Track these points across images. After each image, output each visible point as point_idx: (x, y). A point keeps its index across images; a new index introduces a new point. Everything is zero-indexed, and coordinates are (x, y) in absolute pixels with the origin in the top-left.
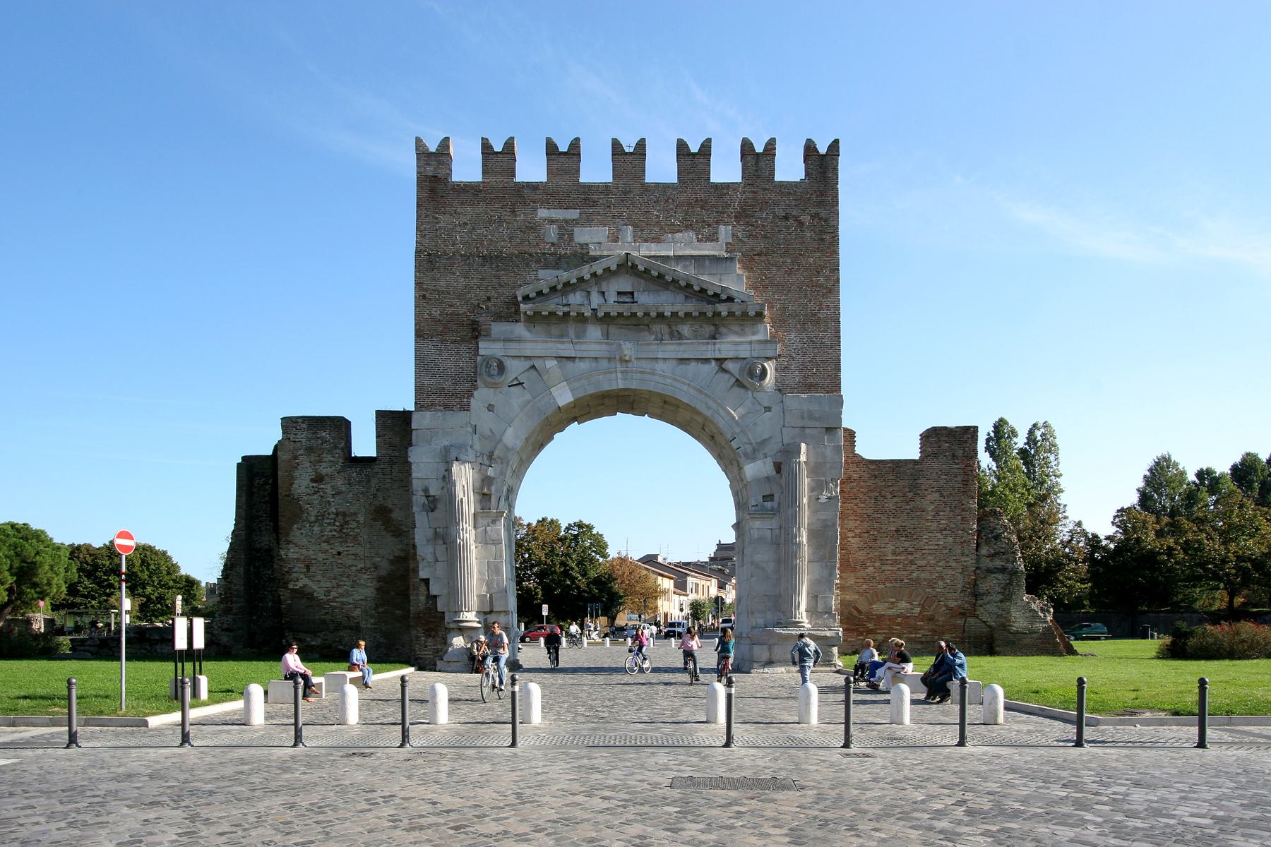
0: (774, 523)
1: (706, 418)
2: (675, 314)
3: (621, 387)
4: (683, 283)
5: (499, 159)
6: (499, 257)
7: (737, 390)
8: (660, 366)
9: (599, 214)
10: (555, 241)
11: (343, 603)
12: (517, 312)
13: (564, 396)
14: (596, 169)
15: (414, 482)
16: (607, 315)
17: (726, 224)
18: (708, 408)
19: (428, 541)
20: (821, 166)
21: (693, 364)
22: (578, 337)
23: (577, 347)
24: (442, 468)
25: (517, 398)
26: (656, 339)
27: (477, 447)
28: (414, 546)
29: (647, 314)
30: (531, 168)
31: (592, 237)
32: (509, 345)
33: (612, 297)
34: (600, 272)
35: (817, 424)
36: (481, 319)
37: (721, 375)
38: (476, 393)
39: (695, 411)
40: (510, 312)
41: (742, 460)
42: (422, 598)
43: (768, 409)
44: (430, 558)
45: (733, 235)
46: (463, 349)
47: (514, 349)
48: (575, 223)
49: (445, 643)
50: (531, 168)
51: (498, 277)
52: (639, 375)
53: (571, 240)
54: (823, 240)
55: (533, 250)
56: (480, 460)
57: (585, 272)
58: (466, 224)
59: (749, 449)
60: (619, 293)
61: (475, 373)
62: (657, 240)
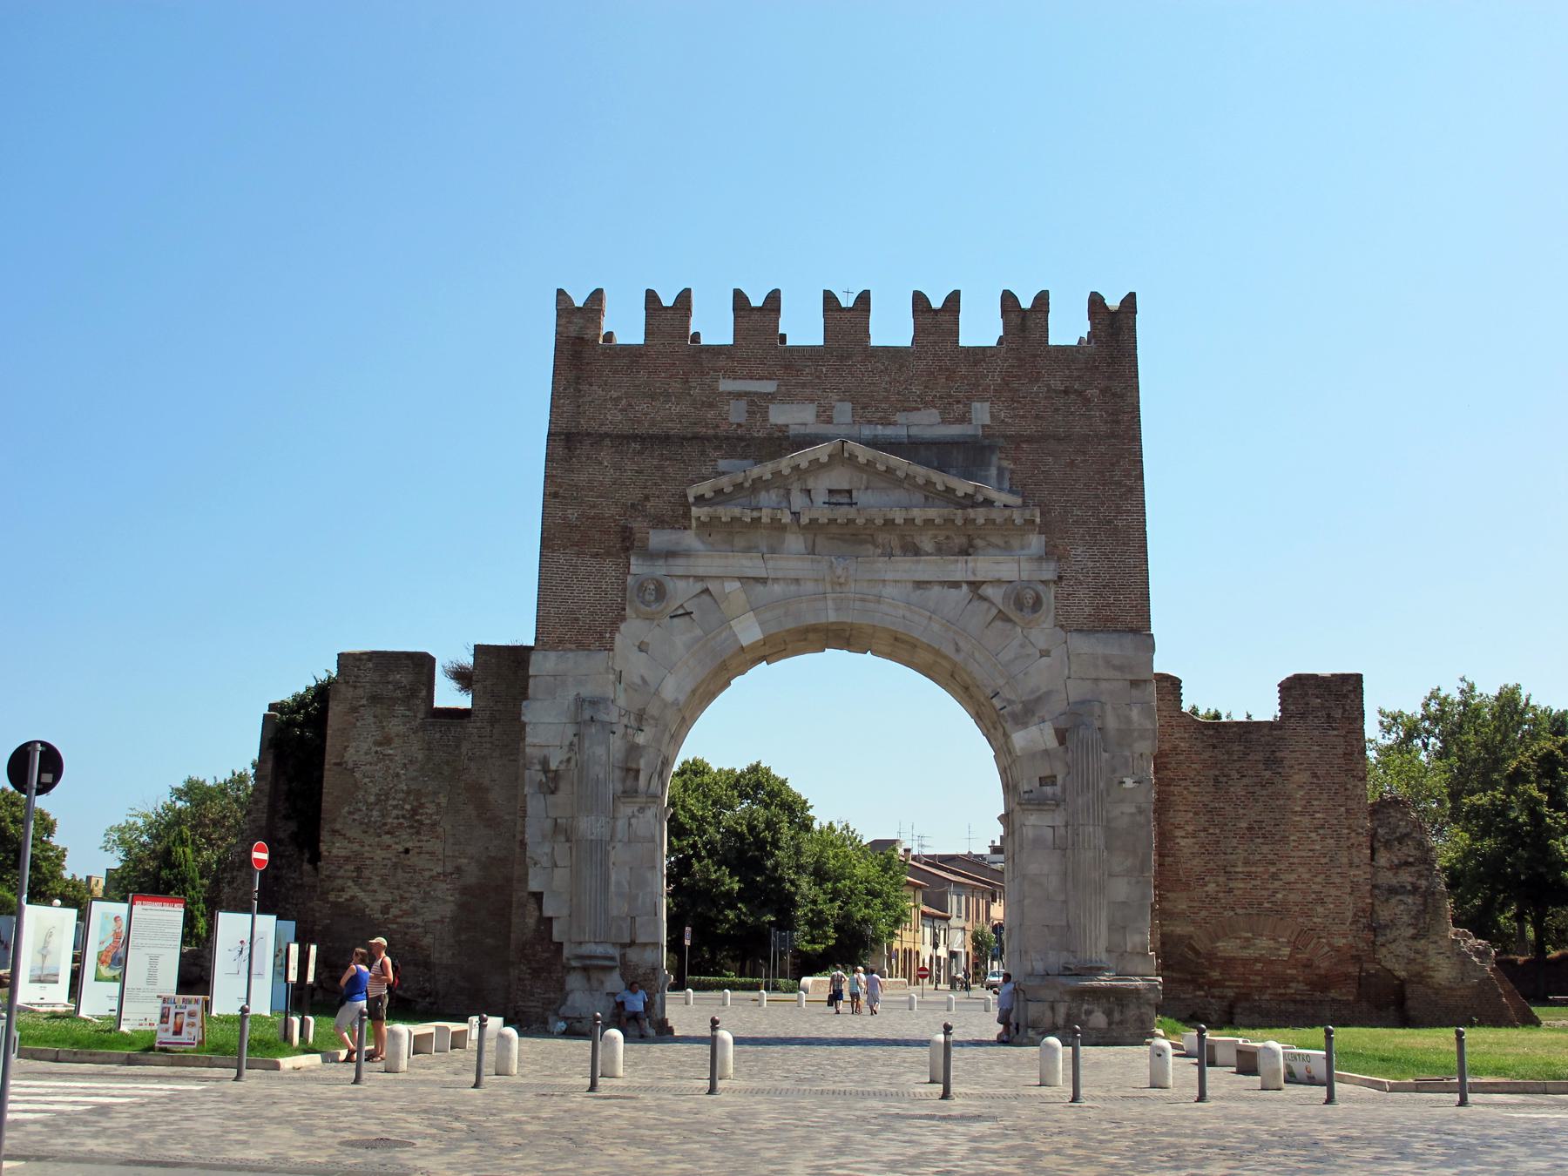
0: (1058, 818)
1: (955, 664)
2: (910, 521)
3: (832, 617)
4: (920, 481)
5: (666, 316)
6: (665, 439)
7: (999, 624)
8: (889, 591)
9: (804, 385)
10: (742, 420)
11: (408, 926)
12: (687, 515)
13: (749, 632)
14: (803, 327)
15: (528, 750)
16: (813, 521)
17: (983, 400)
18: (958, 650)
19: (544, 837)
20: (1111, 325)
21: (937, 589)
22: (773, 551)
23: (771, 564)
24: (570, 731)
25: (681, 636)
26: (883, 555)
27: (622, 701)
28: (523, 844)
29: (870, 521)
30: (714, 326)
31: (794, 416)
32: (671, 561)
33: (821, 497)
34: (804, 465)
35: (1118, 675)
36: (635, 525)
37: (976, 603)
38: (623, 627)
39: (937, 653)
40: (679, 518)
41: (1008, 726)
42: (531, 921)
43: (1045, 653)
44: (545, 862)
45: (992, 416)
46: (609, 566)
47: (679, 566)
48: (770, 397)
49: (562, 988)
50: (714, 326)
51: (659, 468)
52: (858, 604)
53: (766, 419)
54: (1117, 422)
55: (711, 432)
56: (625, 721)
57: (785, 464)
58: (619, 399)
59: (1018, 708)
60: (831, 491)
61: (624, 598)
62: (886, 422)
